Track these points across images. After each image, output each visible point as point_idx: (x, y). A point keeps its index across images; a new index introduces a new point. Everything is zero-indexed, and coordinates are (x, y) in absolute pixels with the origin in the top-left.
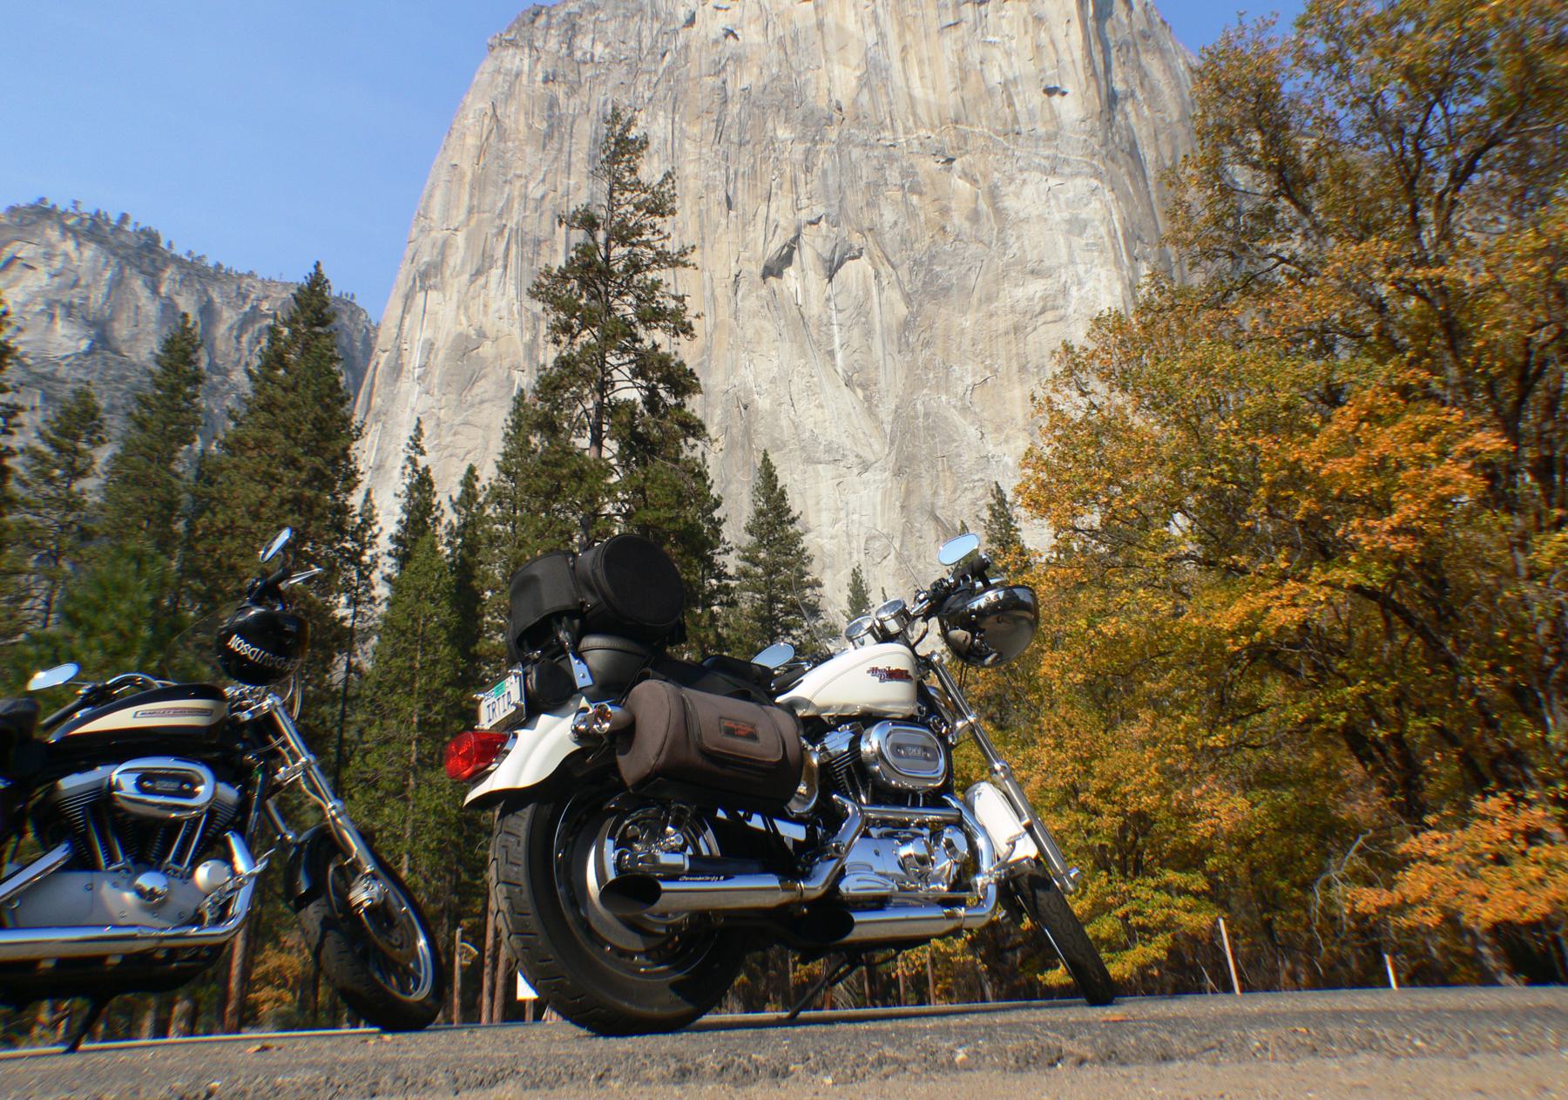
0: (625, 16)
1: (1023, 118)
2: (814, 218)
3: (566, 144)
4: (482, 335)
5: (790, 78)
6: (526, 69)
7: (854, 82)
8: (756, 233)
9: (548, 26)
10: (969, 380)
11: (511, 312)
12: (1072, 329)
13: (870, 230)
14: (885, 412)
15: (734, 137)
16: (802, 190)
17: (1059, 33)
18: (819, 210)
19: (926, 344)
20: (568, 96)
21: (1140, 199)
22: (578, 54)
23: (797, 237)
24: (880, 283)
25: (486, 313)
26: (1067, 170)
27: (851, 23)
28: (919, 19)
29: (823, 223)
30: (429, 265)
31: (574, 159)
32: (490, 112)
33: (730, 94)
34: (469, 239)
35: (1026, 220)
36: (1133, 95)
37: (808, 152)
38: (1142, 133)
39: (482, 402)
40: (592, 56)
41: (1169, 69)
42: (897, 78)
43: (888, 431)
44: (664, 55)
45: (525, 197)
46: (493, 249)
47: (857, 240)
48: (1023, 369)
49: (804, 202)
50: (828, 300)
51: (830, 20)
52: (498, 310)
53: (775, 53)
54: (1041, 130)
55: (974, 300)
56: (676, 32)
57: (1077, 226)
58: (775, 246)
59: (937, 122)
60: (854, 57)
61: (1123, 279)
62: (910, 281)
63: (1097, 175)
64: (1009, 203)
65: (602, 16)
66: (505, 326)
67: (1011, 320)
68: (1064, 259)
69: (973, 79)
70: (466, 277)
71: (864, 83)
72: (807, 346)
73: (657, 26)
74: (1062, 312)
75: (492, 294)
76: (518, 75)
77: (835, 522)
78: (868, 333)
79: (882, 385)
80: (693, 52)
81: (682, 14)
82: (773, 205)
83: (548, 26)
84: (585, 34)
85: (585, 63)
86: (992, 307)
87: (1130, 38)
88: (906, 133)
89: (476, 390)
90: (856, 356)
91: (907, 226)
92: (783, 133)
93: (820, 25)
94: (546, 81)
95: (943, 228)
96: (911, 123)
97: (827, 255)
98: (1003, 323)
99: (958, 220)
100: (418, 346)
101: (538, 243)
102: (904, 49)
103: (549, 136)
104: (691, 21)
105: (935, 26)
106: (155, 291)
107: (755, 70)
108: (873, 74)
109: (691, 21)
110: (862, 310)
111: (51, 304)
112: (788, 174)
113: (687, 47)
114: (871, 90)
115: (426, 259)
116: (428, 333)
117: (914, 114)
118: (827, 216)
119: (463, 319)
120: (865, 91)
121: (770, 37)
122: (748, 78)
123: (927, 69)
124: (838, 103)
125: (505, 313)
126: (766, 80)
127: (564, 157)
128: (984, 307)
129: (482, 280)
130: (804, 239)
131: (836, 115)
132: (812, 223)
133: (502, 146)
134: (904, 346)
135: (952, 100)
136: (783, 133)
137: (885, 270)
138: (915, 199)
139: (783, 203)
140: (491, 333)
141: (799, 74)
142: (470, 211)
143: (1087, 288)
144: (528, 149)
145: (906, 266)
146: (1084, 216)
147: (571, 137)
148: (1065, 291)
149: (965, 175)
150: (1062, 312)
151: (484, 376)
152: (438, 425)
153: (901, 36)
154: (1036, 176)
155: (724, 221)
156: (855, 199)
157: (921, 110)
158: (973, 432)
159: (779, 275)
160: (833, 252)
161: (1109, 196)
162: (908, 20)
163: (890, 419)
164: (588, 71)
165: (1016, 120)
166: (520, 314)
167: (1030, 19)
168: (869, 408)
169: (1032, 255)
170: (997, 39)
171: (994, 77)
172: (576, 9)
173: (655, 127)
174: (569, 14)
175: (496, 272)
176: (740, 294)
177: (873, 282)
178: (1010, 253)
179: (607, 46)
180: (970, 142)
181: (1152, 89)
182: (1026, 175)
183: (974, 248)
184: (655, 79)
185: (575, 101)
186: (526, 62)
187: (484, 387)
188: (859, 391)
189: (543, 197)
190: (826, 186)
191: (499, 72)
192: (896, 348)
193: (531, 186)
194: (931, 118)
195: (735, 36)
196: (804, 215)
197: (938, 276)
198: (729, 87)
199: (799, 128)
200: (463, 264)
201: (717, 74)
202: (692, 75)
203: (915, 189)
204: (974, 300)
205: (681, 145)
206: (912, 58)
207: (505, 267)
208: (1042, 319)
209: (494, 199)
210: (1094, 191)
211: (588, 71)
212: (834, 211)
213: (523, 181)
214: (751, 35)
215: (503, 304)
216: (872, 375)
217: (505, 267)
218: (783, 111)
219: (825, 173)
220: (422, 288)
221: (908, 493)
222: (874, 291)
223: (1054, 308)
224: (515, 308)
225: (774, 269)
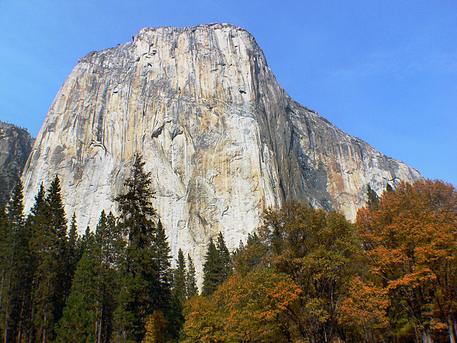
0: (119, 56)
1: (233, 98)
2: (169, 121)
3: (97, 91)
4: (65, 146)
5: (166, 79)
6: (88, 69)
7: (185, 82)
8: (151, 123)
9: (96, 57)
10: (212, 175)
11: (74, 140)
12: (244, 162)
13: (186, 126)
14: (186, 182)
15: (148, 95)
16: (166, 112)
17: (245, 77)
18: (171, 118)
19: (200, 162)
20: (99, 77)
21: (265, 125)
22: (104, 66)
23: (163, 126)
24: (187, 142)
25: (67, 140)
26: (245, 115)
28: (205, 67)
29: (171, 123)
30: (51, 124)
31: (98, 96)
32: (76, 80)
33: (148, 82)
34: (64, 117)
35: (232, 128)
36: (265, 95)
37: (169, 101)
38: (267, 106)
39: (63, 167)
40: (108, 66)
41: (275, 89)
43: (187, 188)
44: (129, 68)
45: (82, 106)
46: (71, 121)
47: (181, 129)
48: (228, 173)
49: (167, 116)
50: (171, 146)
51: (179, 64)
52: (70, 140)
53: (162, 72)
54: (238, 103)
55: (215, 151)
56: (134, 62)
57: (247, 132)
58: (156, 128)
59: (208, 97)
60: (186, 75)
61: (259, 148)
62: (196, 143)
63: (253, 117)
64: (227, 122)
65: (113, 56)
66: (72, 145)
67: (226, 157)
68: (243, 141)
69: (220, 86)
70: (62, 128)
71: (188, 83)
72: (164, 159)
73: (128, 60)
74: (241, 156)
75: (69, 135)
76: (86, 70)
77: (168, 215)
78: (183, 157)
79: (186, 174)
80: (138, 69)
81: (136, 58)
82: (157, 116)
83: (96, 57)
84: (107, 60)
85: (106, 68)
86: (220, 153)
87: (264, 80)
88: (199, 99)
90: (179, 164)
91: (197, 126)
92: (162, 95)
93: (176, 65)
94: (93, 73)
95: (208, 128)
96: (200, 96)
97: (172, 132)
98: (223, 158)
99: (212, 126)
100: (45, 148)
101: (85, 120)
102: (200, 75)
103: (92, 88)
104: (138, 60)
105: (210, 70)
107: (156, 76)
108: (190, 81)
109: (138, 60)
110: (181, 150)
112: (162, 107)
113: (136, 67)
114: (189, 85)
115: (51, 122)
116: (49, 145)
117: (202, 94)
118: (173, 120)
119: (60, 141)
120: (188, 85)
121: (161, 67)
122: (154, 78)
123: (206, 81)
124: (179, 88)
125: (72, 141)
126: (159, 79)
127: (96, 95)
128: (218, 153)
129: (67, 130)
130: (165, 127)
131: (178, 91)
132: (168, 122)
133: (78, 90)
134: (193, 162)
135: (213, 91)
136: (162, 95)
137: (189, 138)
138: (200, 118)
139: (160, 115)
140: (68, 146)
141: (169, 78)
142: (66, 109)
143: (249, 150)
144: (86, 92)
145: (196, 138)
146: (249, 129)
147: (99, 89)
148: (242, 150)
149: (215, 113)
150: (241, 156)
151: (64, 159)
152: (49, 174)
153: (200, 71)
154: (236, 115)
155: (142, 119)
156: (182, 116)
157: (204, 93)
158: (212, 191)
159: (157, 137)
160: (174, 131)
161: (257, 124)
162: (202, 67)
163: (187, 184)
164: (106, 71)
165: (231, 99)
166: (77, 141)
167: (237, 71)
168: (181, 180)
169: (233, 139)
170: (227, 75)
171: (226, 86)
172: (105, 53)
173: (124, 89)
174: (103, 54)
175: (71, 128)
176: (144, 141)
177: (185, 141)
178: (227, 137)
179: (113, 64)
180: (217, 103)
181: (270, 94)
182: (233, 115)
183: (216, 134)
184: (126, 75)
185: (101, 79)
186: (89, 67)
187: (64, 163)
188: (178, 174)
189: (88, 106)
190: (174, 111)
191: (80, 69)
192: (191, 163)
193: (85, 103)
194: (207, 96)
195: (151, 66)
196: (166, 120)
197: (205, 142)
198: (148, 80)
199: (167, 93)
200: (62, 124)
201: (144, 76)
202: (137, 75)
203: (200, 115)
204: (215, 151)
205: (131, 95)
207: (74, 127)
208: (235, 158)
209: (73, 106)
210: (252, 122)
211: (106, 71)
212: (175, 119)
213: (83, 101)
214: (156, 66)
215: (72, 138)
216: (183, 170)
217: (74, 127)
218: (163, 88)
219: (173, 107)
220: (49, 131)
221: (192, 208)
222: (185, 144)
223: (239, 155)
224: (76, 139)
225: (156, 135)
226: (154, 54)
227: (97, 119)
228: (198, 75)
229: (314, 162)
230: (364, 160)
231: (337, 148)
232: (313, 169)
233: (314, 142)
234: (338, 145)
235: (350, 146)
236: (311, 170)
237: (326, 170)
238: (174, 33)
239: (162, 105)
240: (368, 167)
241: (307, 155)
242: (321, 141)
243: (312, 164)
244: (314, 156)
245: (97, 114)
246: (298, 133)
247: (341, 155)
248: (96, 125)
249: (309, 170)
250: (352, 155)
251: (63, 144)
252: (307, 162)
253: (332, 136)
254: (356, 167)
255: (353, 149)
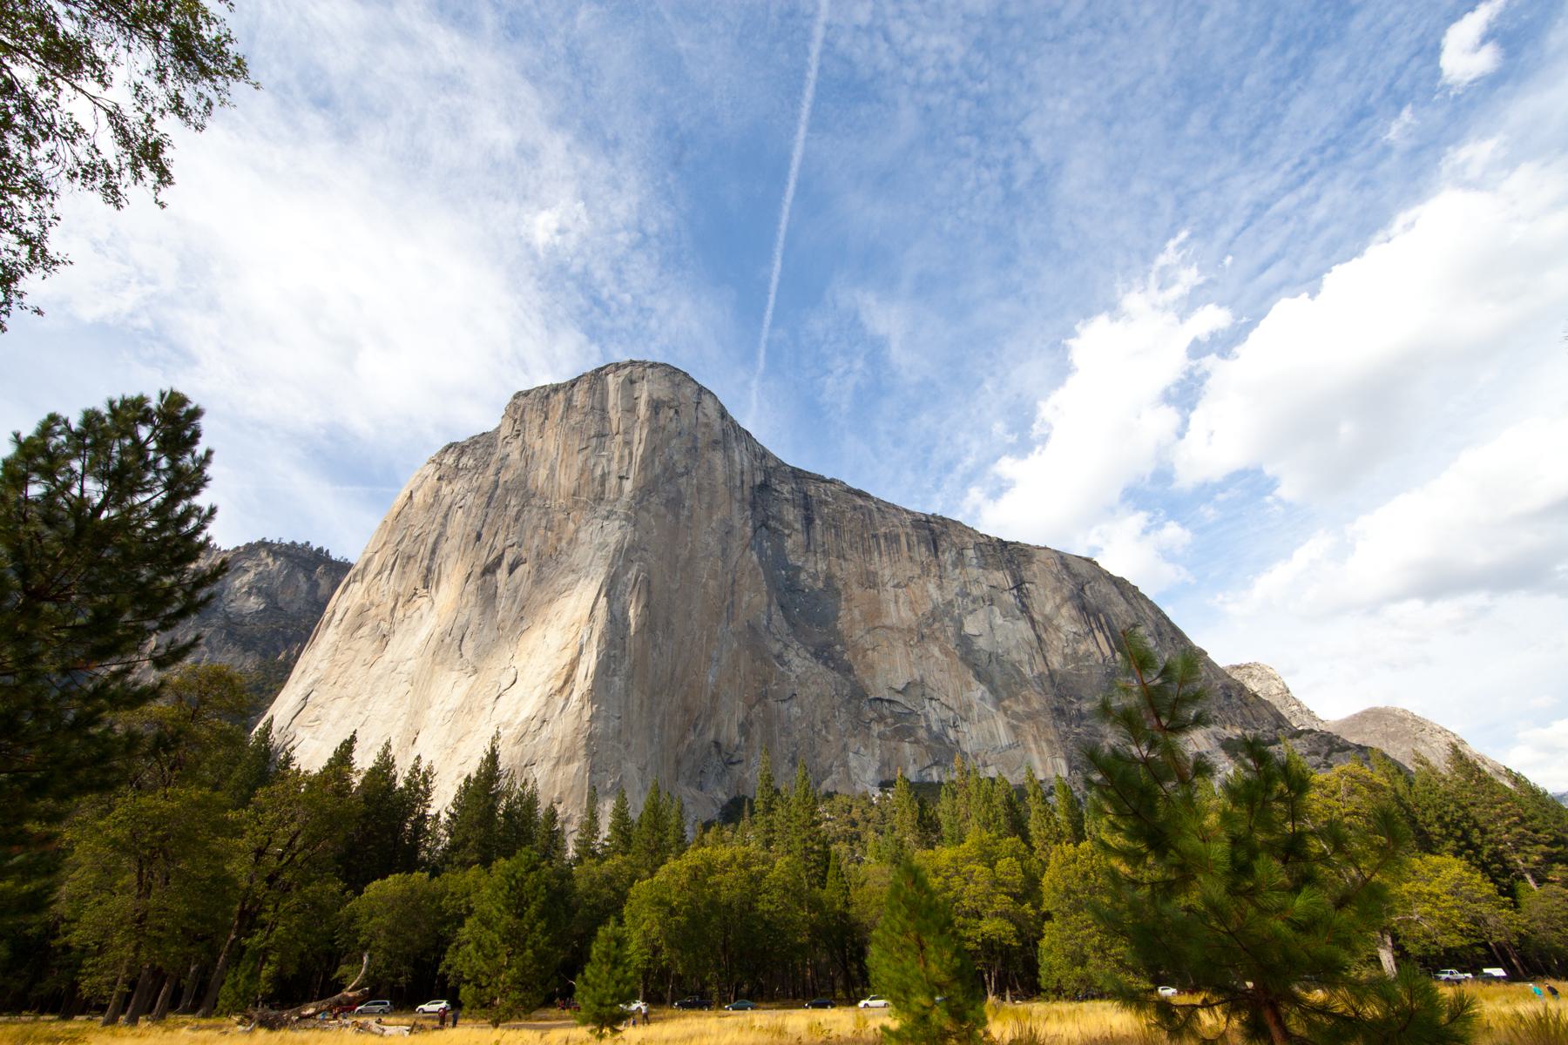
1: (607, 491)
9: (453, 453)
18: (515, 540)
23: (503, 554)
27: (551, 449)
42: (557, 475)
47: (524, 555)
49: (511, 536)
60: (548, 466)
89: (360, 632)
105: (577, 449)
106: (309, 578)
110: (516, 591)
111: (250, 588)
129: (379, 577)
130: (506, 554)
138: (549, 533)
165: (603, 492)
177: (526, 575)
187: (365, 630)
196: (509, 543)
206: (564, 464)
207: (392, 570)
226: (518, 435)
227: (427, 554)
228: (559, 460)
229: (815, 577)
230: (941, 557)
231: (872, 542)
232: (812, 589)
233: (819, 537)
234: (875, 536)
235: (907, 534)
236: (807, 590)
237: (841, 587)
238: (552, 395)
239: (507, 520)
240: (950, 568)
241: (800, 564)
242: (837, 535)
243: (810, 580)
244: (816, 563)
245: (430, 546)
246: (781, 528)
247: (880, 554)
248: (425, 563)
249: (804, 591)
250: (909, 550)
251: (371, 598)
252: (798, 577)
253: (863, 521)
254: (919, 572)
255: (915, 538)
